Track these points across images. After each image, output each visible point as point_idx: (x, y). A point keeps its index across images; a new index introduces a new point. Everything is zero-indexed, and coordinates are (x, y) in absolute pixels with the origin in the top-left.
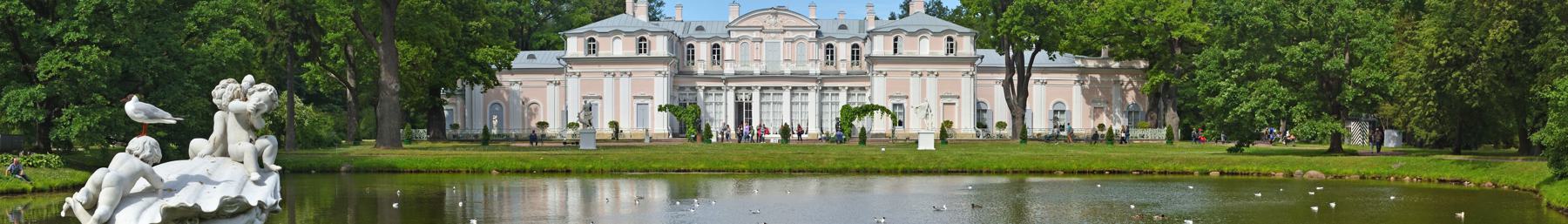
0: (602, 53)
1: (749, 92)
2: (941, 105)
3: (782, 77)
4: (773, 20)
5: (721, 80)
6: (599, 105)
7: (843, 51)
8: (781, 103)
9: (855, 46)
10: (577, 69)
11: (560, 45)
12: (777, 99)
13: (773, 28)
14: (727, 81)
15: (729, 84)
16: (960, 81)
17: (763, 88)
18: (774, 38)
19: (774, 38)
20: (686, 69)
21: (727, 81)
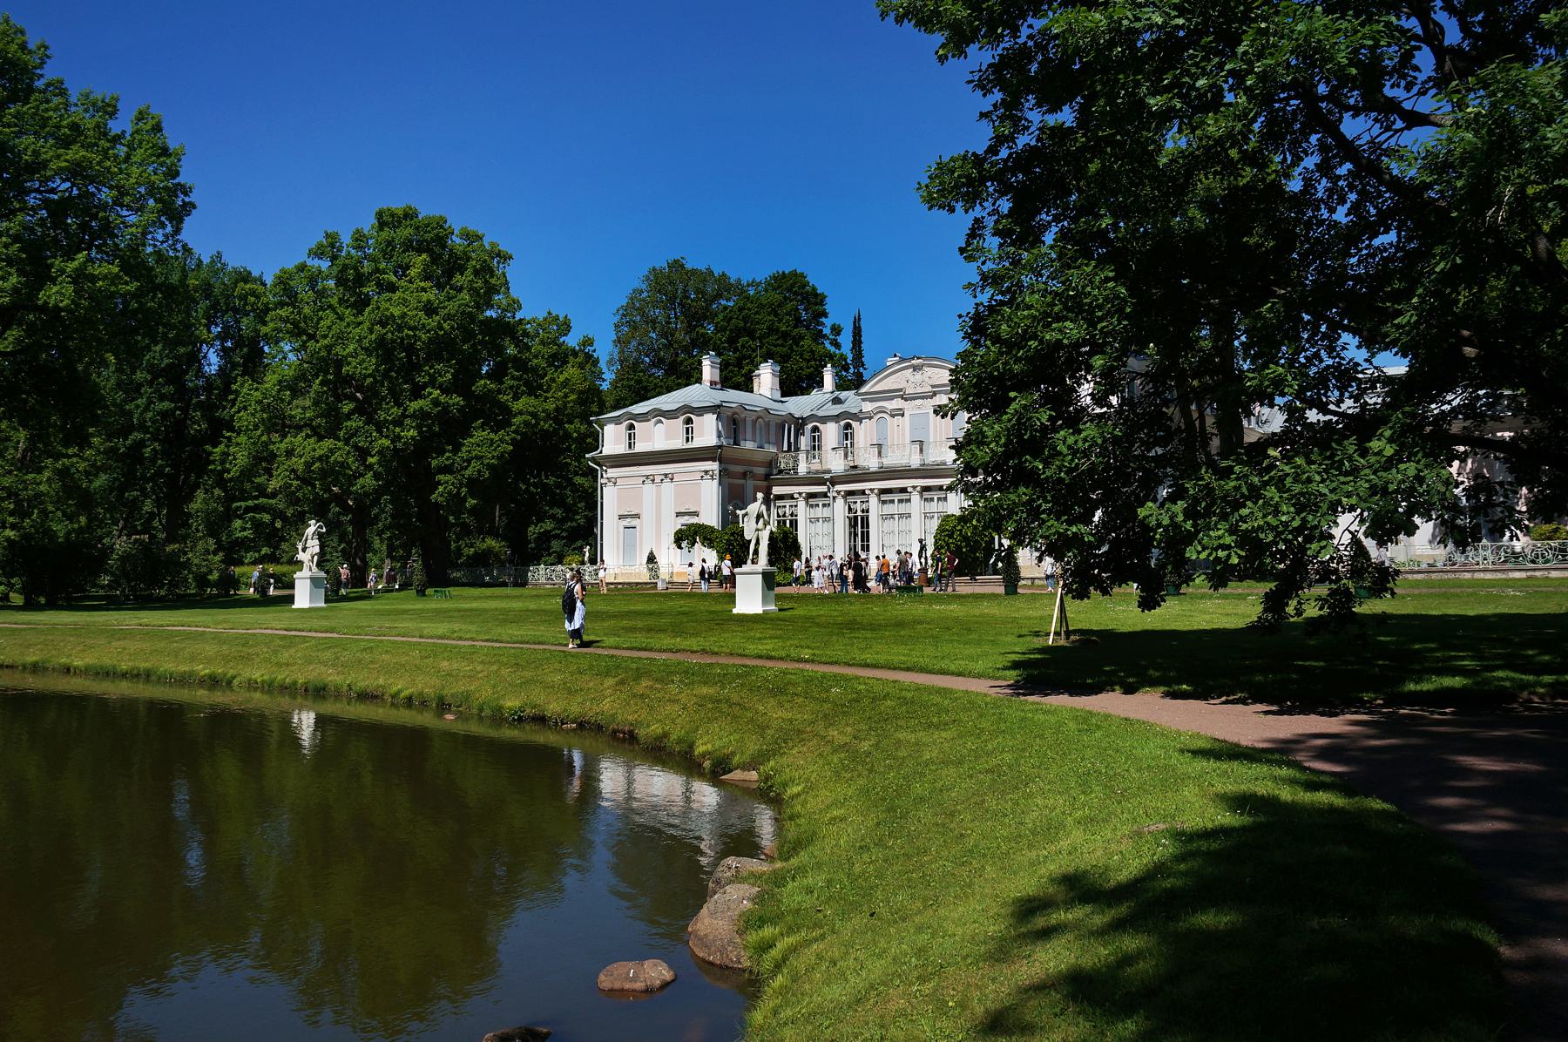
1: (864, 498)
5: (822, 482)
8: (909, 516)
12: (903, 508)
13: (919, 390)
14: (834, 481)
15: (838, 487)
21: (834, 481)
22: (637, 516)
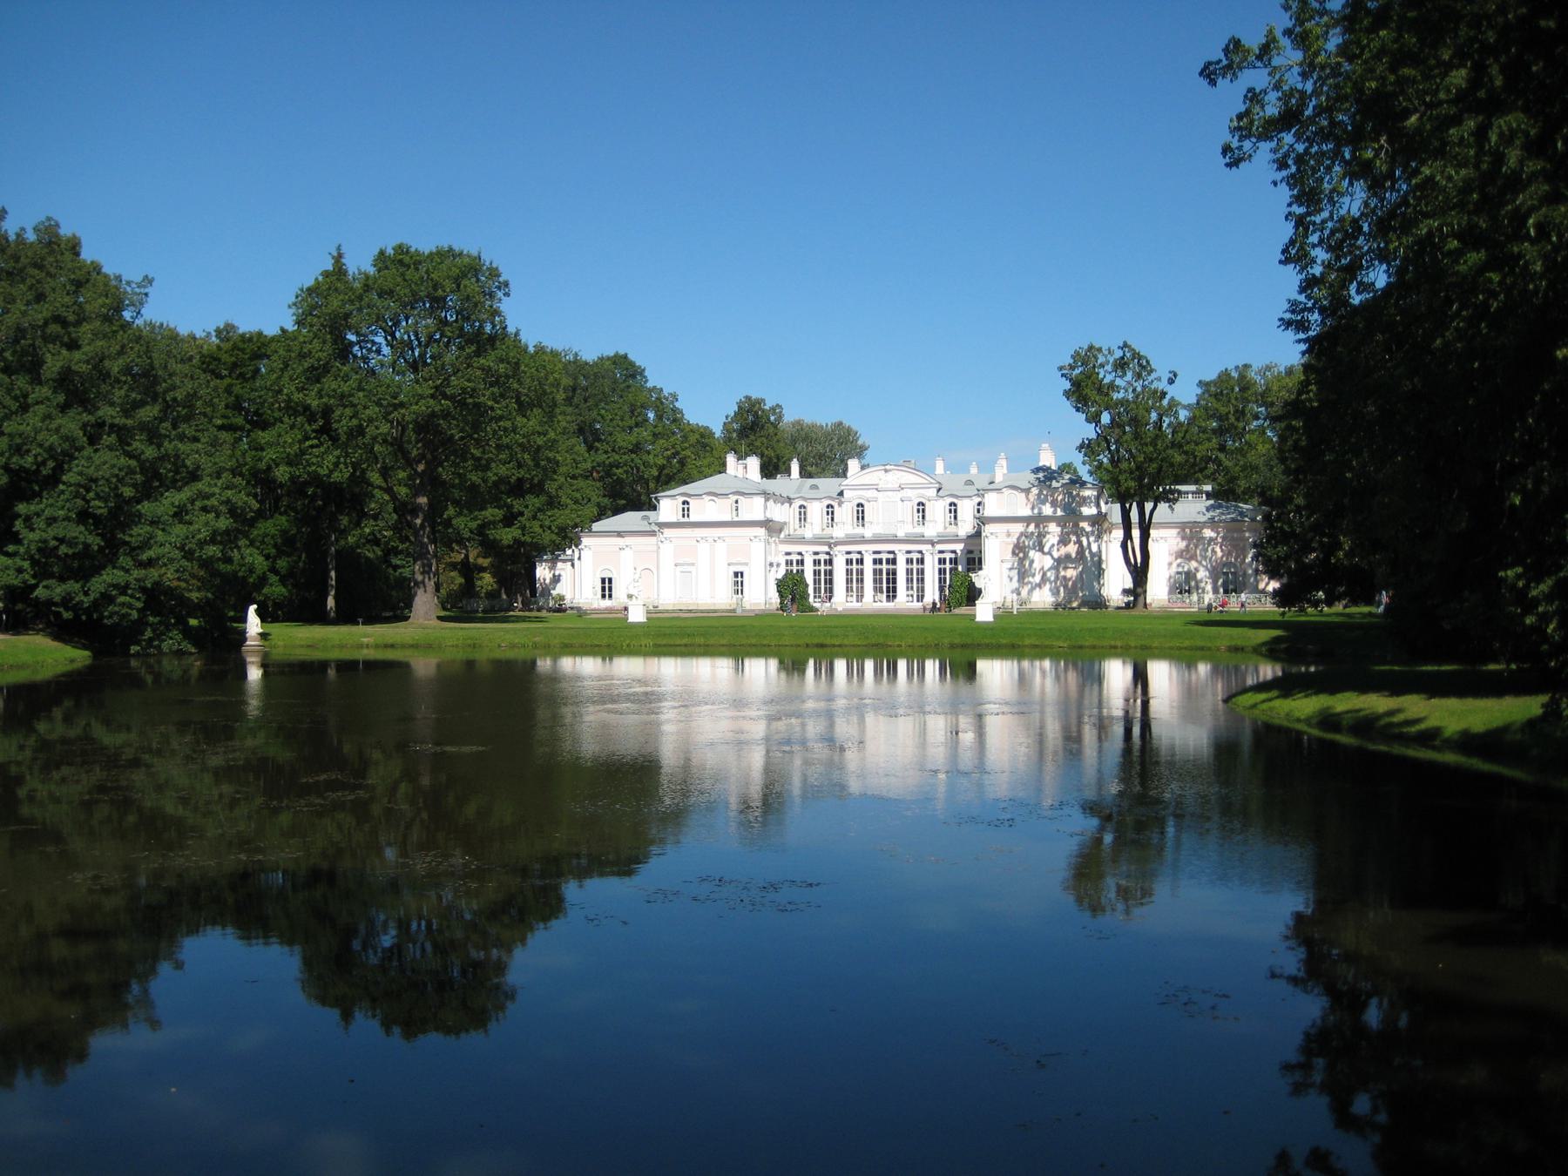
0: (694, 518)
6: (694, 573)
7: (967, 509)
10: (668, 532)
11: (654, 508)
14: (836, 544)
15: (839, 548)
17: (875, 552)
20: (800, 532)
22: (693, 564)
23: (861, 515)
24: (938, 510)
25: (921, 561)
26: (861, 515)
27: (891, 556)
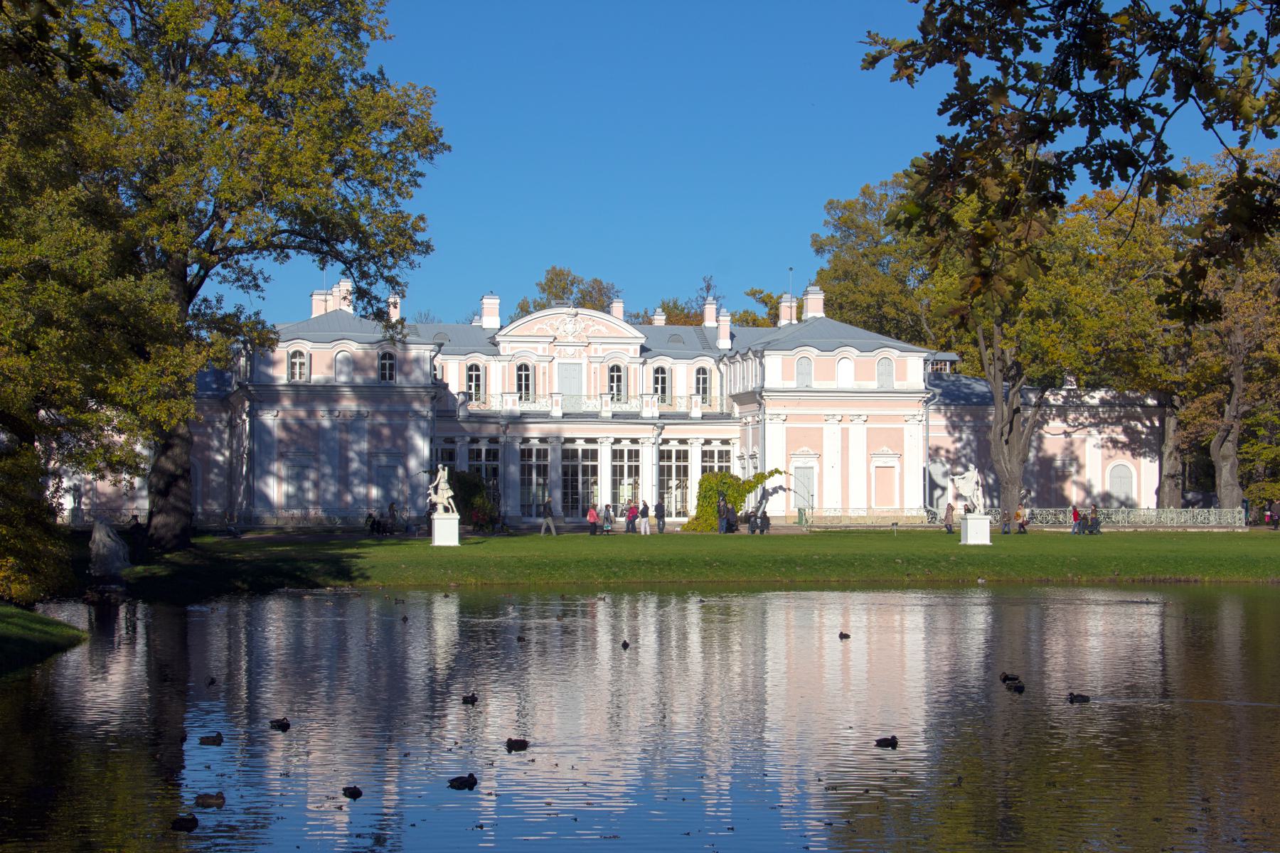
2: (873, 470)
3: (593, 417)
4: (570, 327)
9: (702, 371)
13: (570, 339)
16: (902, 429)
18: (573, 356)
19: (573, 356)
23: (524, 379)
24: (640, 378)
25: (634, 455)
26: (524, 379)
27: (590, 447)
